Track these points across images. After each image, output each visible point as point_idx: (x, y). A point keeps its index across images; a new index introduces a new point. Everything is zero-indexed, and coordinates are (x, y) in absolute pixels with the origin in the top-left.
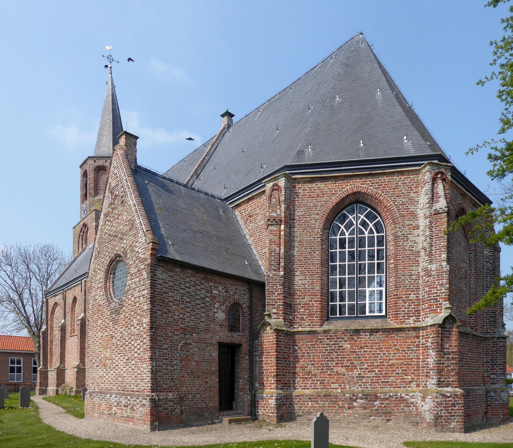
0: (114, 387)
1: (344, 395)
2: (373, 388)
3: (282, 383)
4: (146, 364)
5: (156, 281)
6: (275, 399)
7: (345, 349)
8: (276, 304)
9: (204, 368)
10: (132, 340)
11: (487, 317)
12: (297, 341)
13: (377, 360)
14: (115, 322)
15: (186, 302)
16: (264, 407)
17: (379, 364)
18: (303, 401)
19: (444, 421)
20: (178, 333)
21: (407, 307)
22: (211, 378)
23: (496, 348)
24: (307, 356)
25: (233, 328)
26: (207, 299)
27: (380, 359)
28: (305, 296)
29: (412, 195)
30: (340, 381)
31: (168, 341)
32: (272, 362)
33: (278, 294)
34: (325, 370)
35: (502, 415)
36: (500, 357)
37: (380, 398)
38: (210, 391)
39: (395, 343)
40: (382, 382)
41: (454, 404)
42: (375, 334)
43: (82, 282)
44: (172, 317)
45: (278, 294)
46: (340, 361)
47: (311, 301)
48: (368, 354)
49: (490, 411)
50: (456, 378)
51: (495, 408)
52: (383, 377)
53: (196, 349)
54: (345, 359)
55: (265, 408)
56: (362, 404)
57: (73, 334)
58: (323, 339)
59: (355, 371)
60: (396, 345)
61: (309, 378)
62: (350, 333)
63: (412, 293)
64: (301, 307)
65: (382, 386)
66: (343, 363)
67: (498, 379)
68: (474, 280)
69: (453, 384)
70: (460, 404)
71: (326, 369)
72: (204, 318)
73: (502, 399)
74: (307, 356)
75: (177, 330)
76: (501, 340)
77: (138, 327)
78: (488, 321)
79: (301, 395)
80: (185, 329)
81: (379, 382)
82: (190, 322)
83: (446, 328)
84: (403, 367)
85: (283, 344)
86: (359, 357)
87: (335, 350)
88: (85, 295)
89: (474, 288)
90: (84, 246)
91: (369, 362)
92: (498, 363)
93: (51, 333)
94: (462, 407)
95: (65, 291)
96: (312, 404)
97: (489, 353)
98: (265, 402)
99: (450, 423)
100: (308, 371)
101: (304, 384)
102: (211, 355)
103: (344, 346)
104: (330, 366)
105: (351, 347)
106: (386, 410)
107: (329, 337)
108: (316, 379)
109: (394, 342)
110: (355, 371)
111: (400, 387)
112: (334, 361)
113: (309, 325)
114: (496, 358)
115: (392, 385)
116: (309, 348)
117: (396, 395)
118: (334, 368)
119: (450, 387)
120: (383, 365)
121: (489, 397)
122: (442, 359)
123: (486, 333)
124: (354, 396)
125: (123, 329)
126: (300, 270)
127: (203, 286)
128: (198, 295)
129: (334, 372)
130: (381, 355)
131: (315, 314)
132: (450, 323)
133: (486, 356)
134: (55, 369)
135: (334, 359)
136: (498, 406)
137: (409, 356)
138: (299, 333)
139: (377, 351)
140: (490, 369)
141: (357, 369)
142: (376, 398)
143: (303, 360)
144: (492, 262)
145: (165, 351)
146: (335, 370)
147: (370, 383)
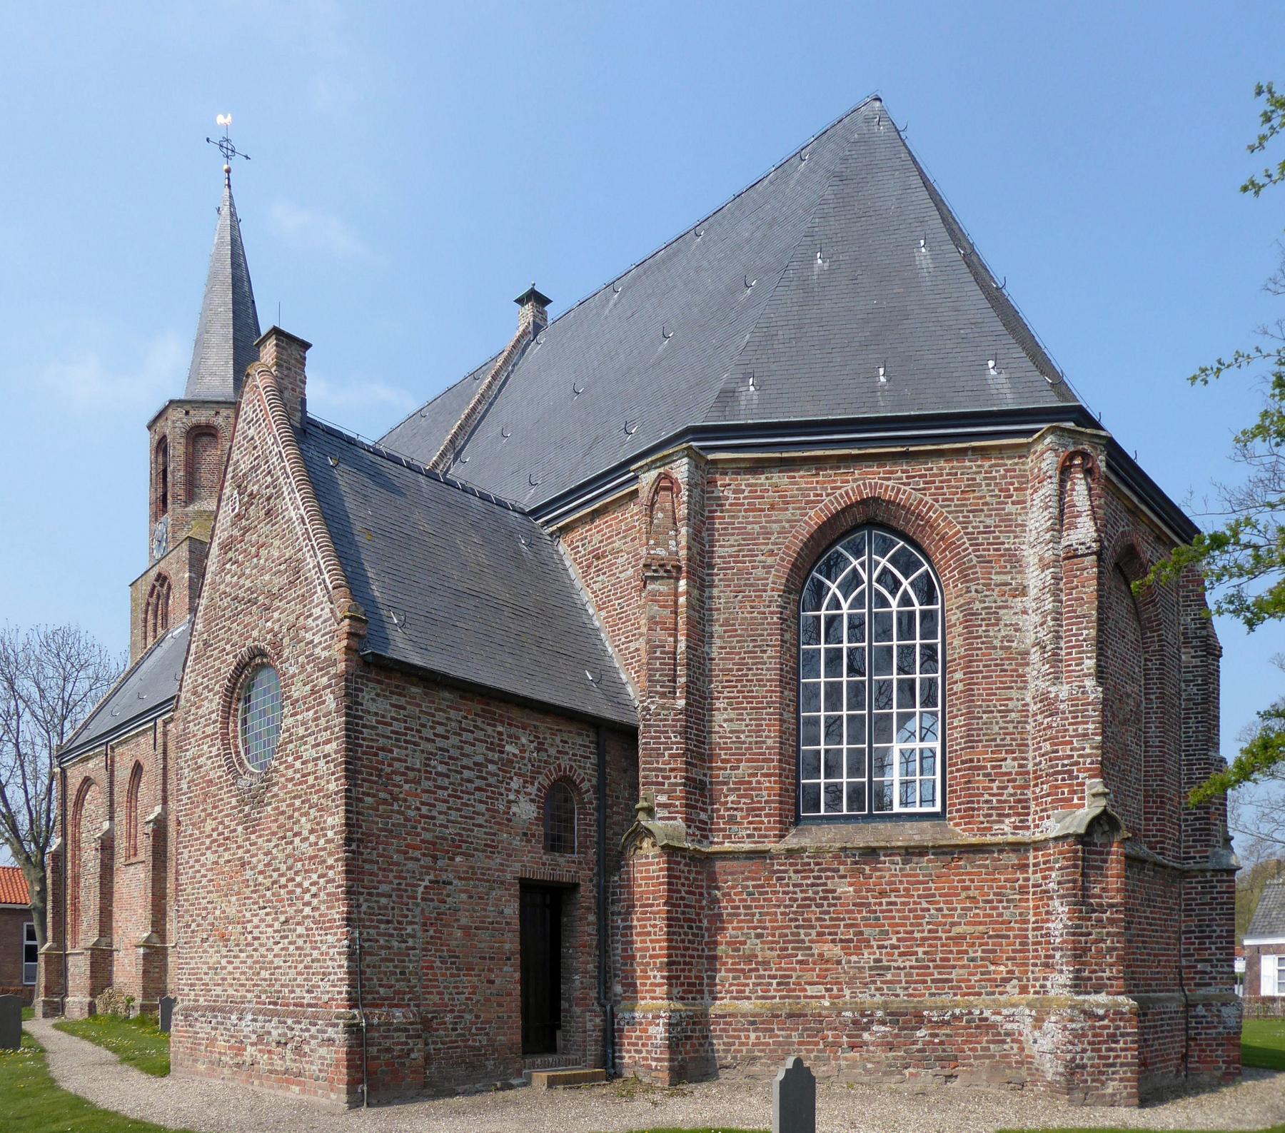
0: (249, 995)
1: (839, 1015)
2: (910, 995)
3: (683, 984)
4: (336, 934)
5: (361, 718)
6: (664, 1024)
7: (840, 898)
8: (667, 782)
9: (483, 945)
10: (297, 873)
11: (1187, 820)
12: (720, 878)
13: (921, 925)
14: (251, 825)
15: (438, 774)
16: (637, 1045)
17: (926, 934)
18: (734, 1030)
19: (1089, 1079)
20: (417, 854)
21: (995, 791)
22: (501, 970)
23: (1209, 896)
24: (746, 915)
25: (556, 842)
26: (491, 767)
27: (928, 923)
28: (740, 761)
29: (1010, 508)
30: (828, 979)
31: (391, 875)
32: (657, 929)
33: (671, 756)
34: (790, 952)
35: (1224, 1062)
36: (1221, 919)
37: (930, 1021)
38: (500, 1005)
39: (967, 883)
40: (933, 981)
41: (1114, 1035)
42: (915, 859)
43: (155, 724)
44: (402, 813)
45: (671, 756)
46: (827, 927)
47: (755, 775)
48: (898, 911)
49: (1196, 1054)
50: (1119, 972)
51: (1208, 1045)
52: (935, 967)
53: (464, 896)
54: (842, 923)
55: (640, 1047)
56: (885, 1036)
57: (133, 860)
58: (785, 871)
59: (866, 952)
60: (968, 888)
61: (750, 970)
62: (854, 855)
63: (1010, 756)
64: (729, 790)
65: (933, 991)
66: (836, 934)
67: (1214, 974)
68: (1156, 727)
69: (1112, 986)
70: (1128, 1034)
71: (793, 949)
72: (483, 815)
73: (1225, 1022)
74: (746, 915)
75: (415, 848)
76: (1222, 876)
77: (312, 838)
78: (1189, 828)
79: (731, 1015)
80: (434, 844)
81: (925, 982)
82: (446, 827)
83: (1095, 845)
84: (987, 944)
85: (683, 885)
86: (877, 919)
87: (814, 899)
88: (165, 758)
89: (1156, 747)
90: (160, 631)
91: (901, 929)
92: (1214, 935)
93: (74, 856)
94: (1133, 1042)
95: (112, 748)
96: (758, 1038)
97: (1194, 910)
98: (638, 1033)
99: (1103, 1083)
100: (747, 952)
101: (738, 985)
102: (502, 912)
103: (839, 890)
104: (803, 941)
105: (855, 891)
106: (944, 1051)
107: (799, 867)
108: (767, 973)
109: (964, 881)
110: (866, 952)
111: (979, 994)
112: (812, 927)
113: (749, 836)
114: (1209, 920)
115: (960, 988)
116: (749, 894)
117: (970, 1013)
118: (813, 945)
119: (1104, 994)
120: (936, 938)
121: (1193, 1017)
122: (1084, 923)
123: (1185, 859)
124: (863, 1015)
125: (272, 844)
126: (726, 694)
127: (480, 734)
128: (467, 756)
129: (813, 955)
130: (932, 912)
131: (764, 809)
132: (1104, 833)
133: (1186, 916)
134: (86, 949)
135: (814, 923)
136: (1214, 1039)
137: (1000, 915)
138: (725, 855)
139: (920, 903)
140: (1195, 949)
141: (872, 947)
142: (920, 1020)
143: (735, 924)
144: (1200, 682)
145: (383, 901)
146: (816, 952)
147: (904, 984)
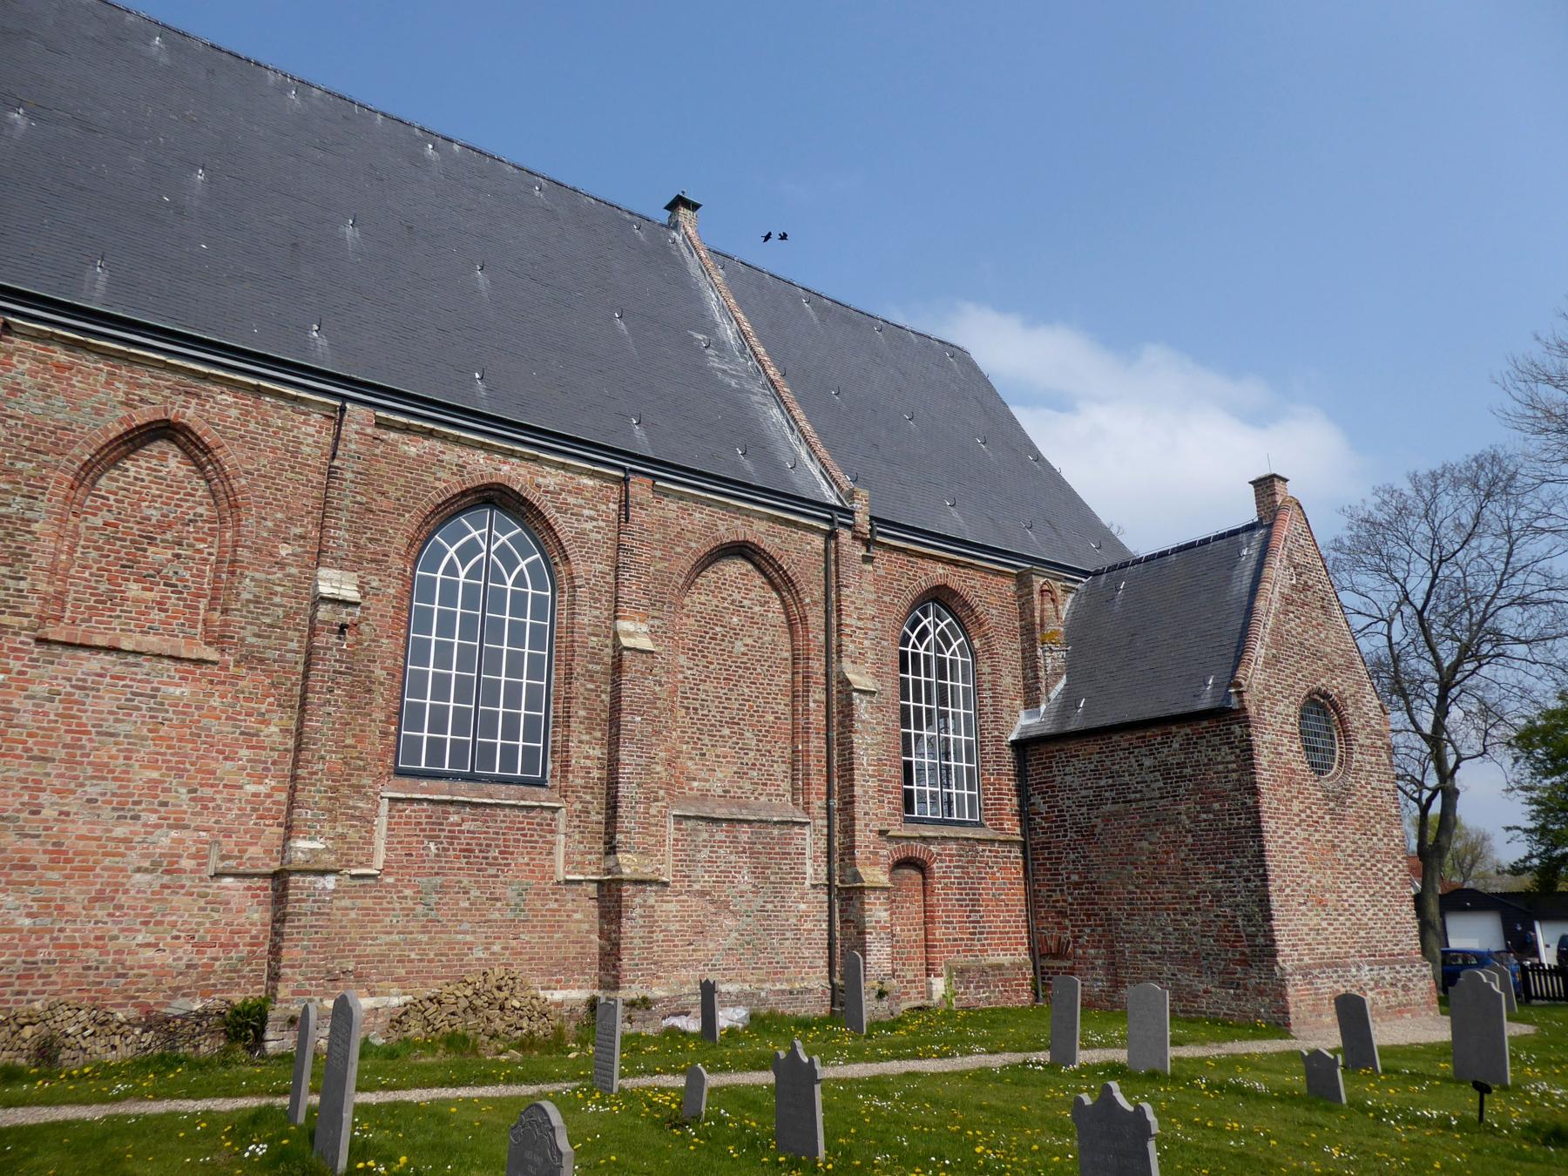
0: (1352, 951)
10: (1378, 861)
14: (1339, 819)
77: (1386, 840)
